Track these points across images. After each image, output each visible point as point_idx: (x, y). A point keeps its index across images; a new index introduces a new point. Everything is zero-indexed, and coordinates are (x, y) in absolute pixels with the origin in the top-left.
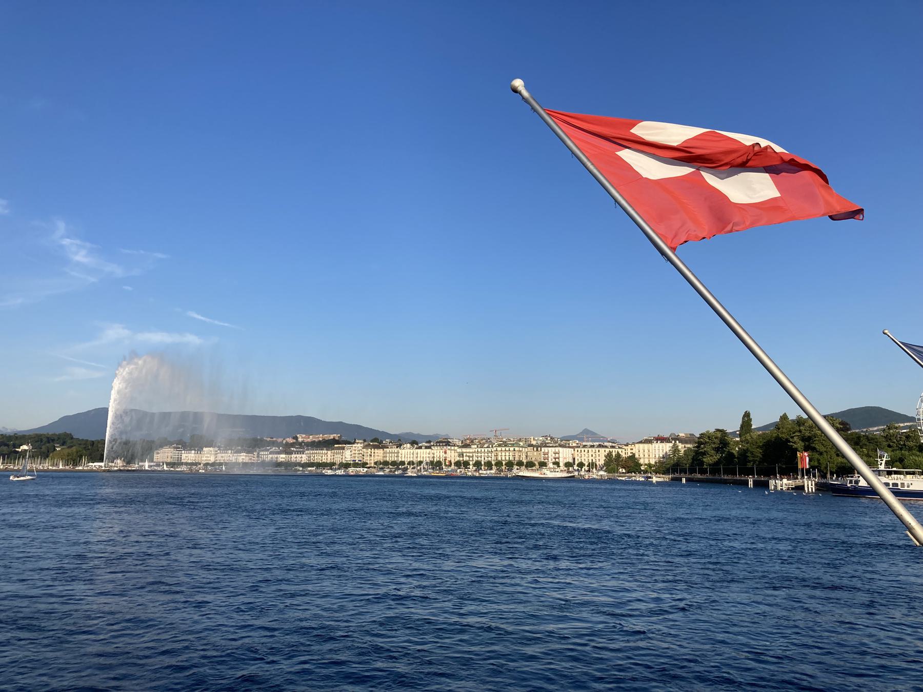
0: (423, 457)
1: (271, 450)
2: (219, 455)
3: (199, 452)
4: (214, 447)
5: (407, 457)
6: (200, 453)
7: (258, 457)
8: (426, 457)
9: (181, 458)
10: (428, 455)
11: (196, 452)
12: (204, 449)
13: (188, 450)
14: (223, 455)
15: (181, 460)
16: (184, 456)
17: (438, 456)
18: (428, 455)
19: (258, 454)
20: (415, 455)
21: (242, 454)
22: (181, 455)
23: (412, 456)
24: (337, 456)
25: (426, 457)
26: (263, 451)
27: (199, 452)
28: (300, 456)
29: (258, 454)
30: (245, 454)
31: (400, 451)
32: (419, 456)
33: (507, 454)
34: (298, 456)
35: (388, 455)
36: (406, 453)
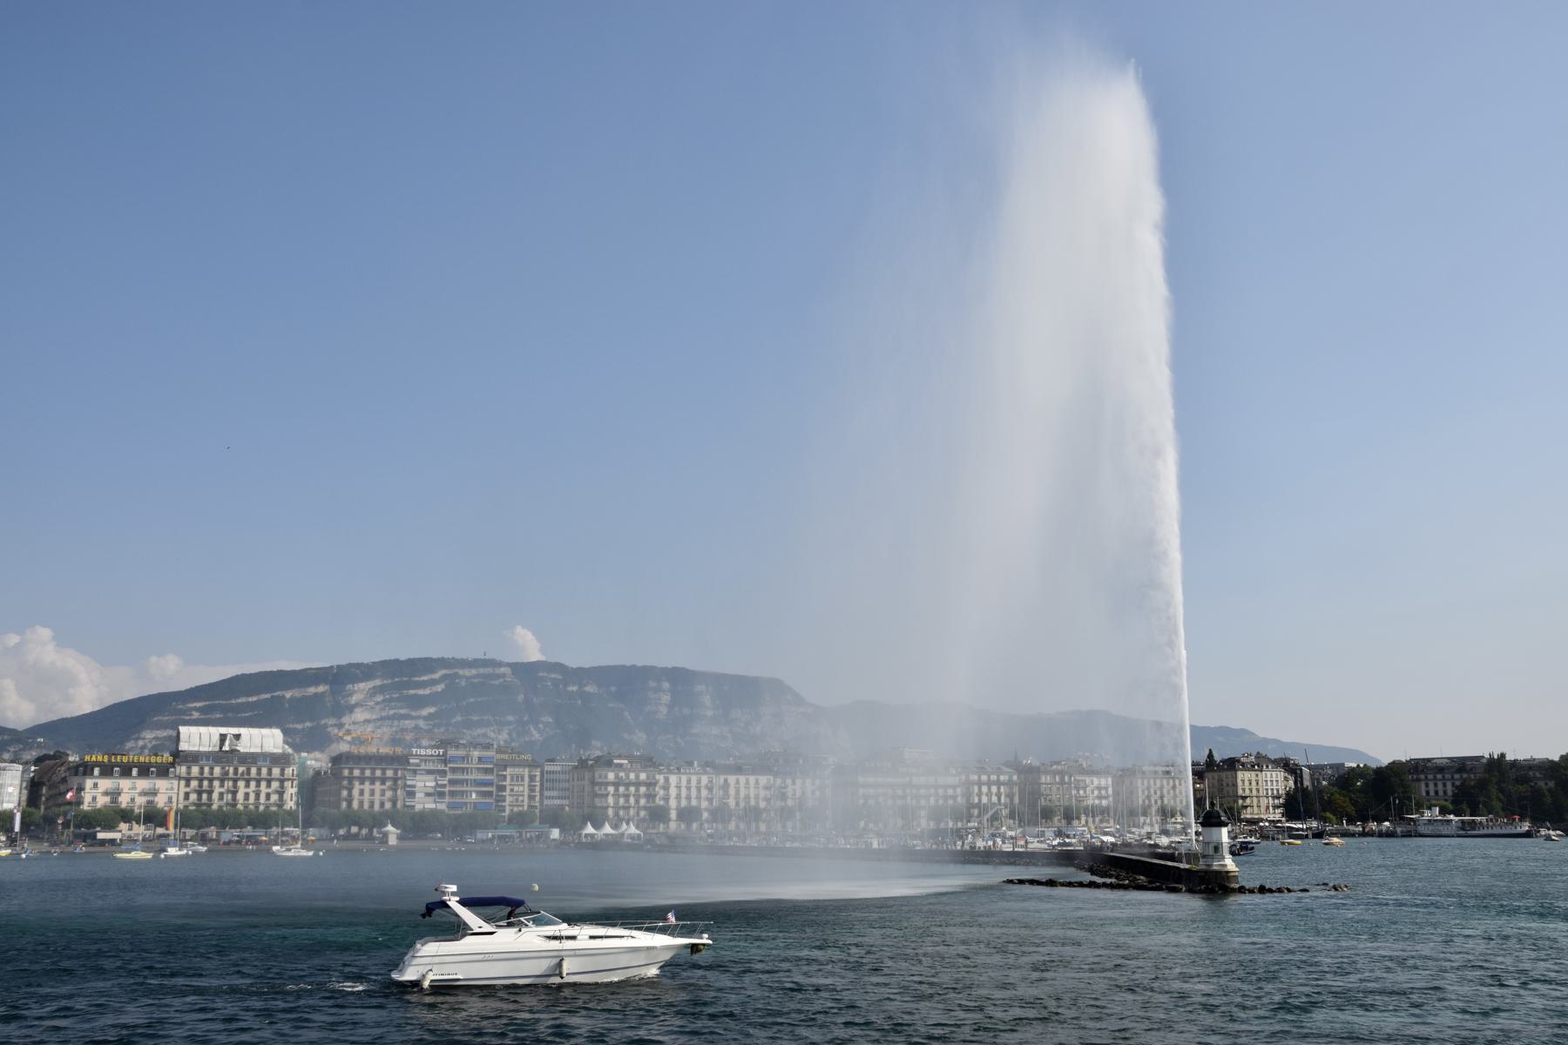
0: (747, 797)
5: (689, 798)
8: (757, 797)
10: (762, 793)
17: (798, 794)
18: (762, 793)
20: (717, 793)
23: (704, 793)
24: (367, 786)
25: (757, 797)
28: (143, 784)
31: (661, 778)
32: (732, 791)
33: (994, 789)
34: (125, 784)
35: (611, 789)
36: (684, 783)
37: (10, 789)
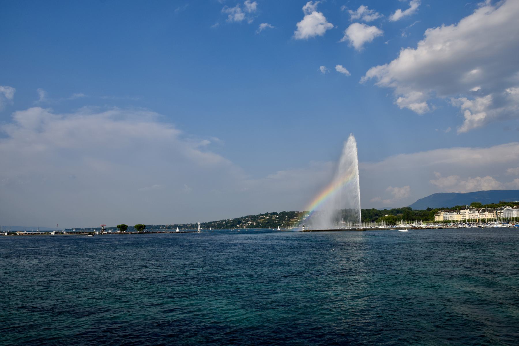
1: (505, 209)
2: (471, 215)
3: (459, 213)
4: (467, 209)
6: (460, 214)
7: (496, 214)
9: (448, 218)
11: (457, 213)
12: (462, 211)
13: (451, 213)
14: (473, 214)
15: (448, 219)
16: (449, 217)
19: (497, 212)
21: (486, 213)
22: (448, 216)
26: (499, 210)
27: (459, 213)
29: (497, 212)
30: (488, 213)
37: (514, 214)
